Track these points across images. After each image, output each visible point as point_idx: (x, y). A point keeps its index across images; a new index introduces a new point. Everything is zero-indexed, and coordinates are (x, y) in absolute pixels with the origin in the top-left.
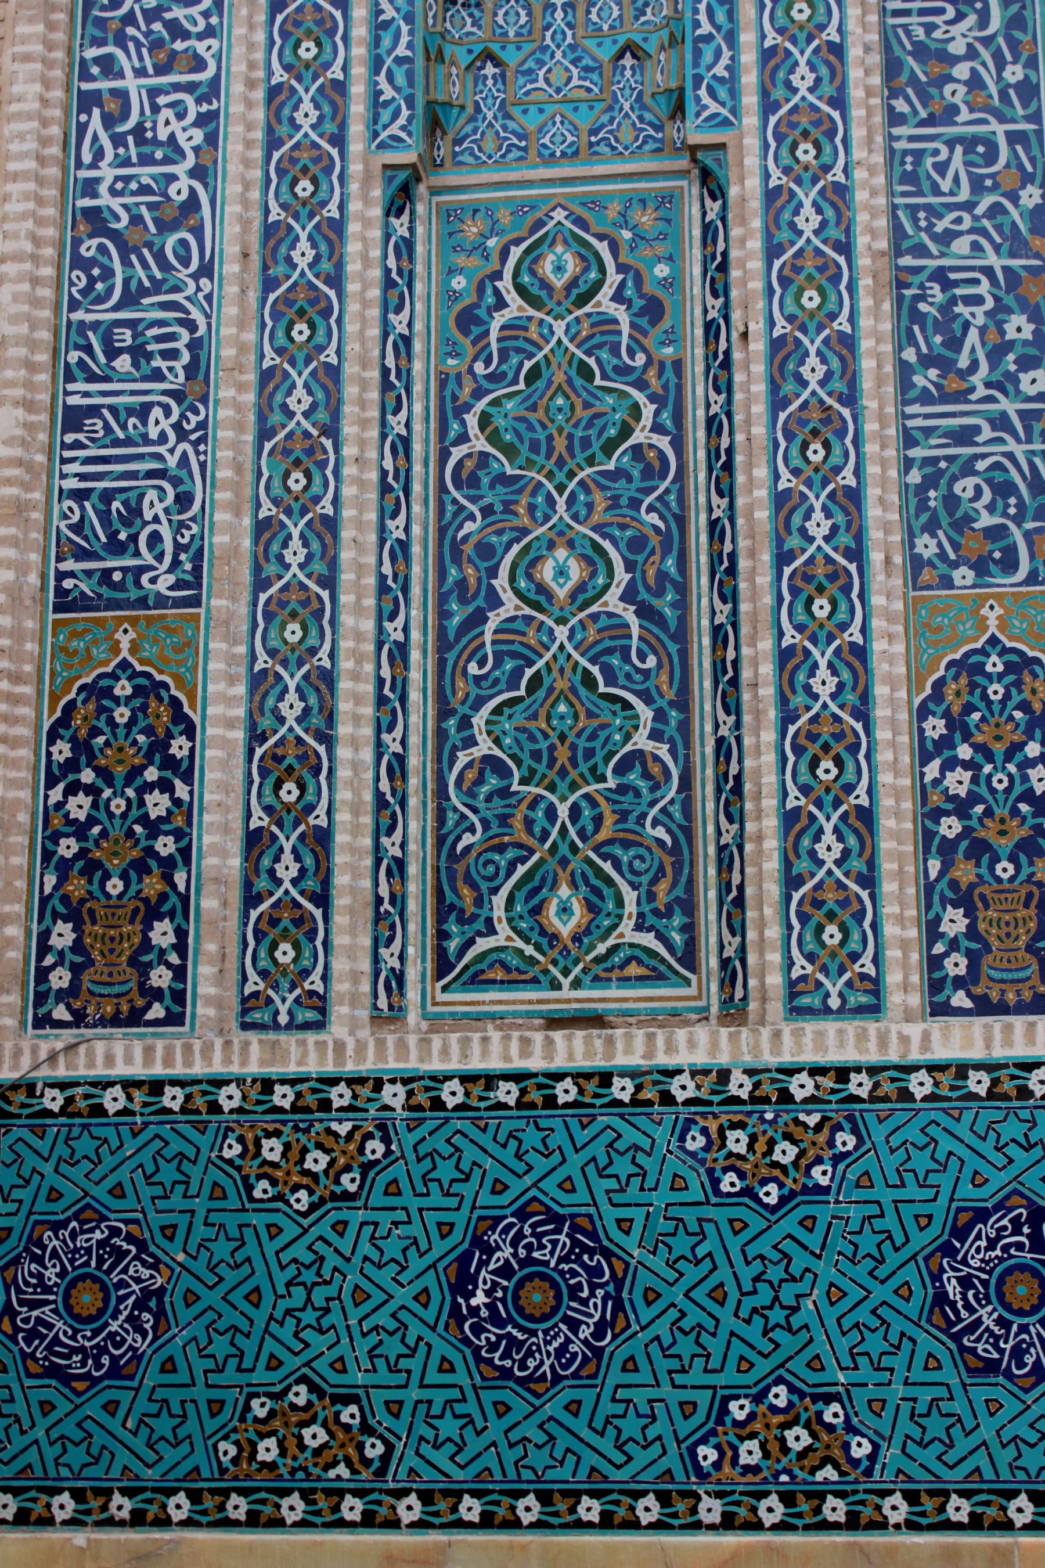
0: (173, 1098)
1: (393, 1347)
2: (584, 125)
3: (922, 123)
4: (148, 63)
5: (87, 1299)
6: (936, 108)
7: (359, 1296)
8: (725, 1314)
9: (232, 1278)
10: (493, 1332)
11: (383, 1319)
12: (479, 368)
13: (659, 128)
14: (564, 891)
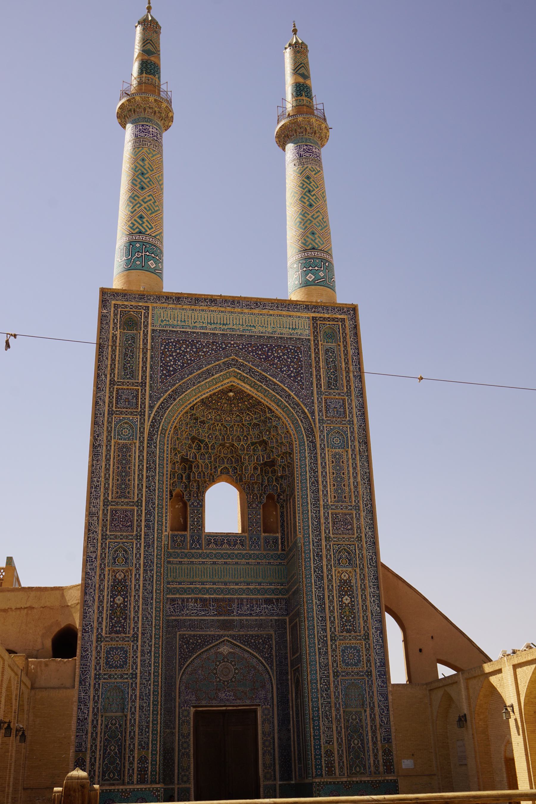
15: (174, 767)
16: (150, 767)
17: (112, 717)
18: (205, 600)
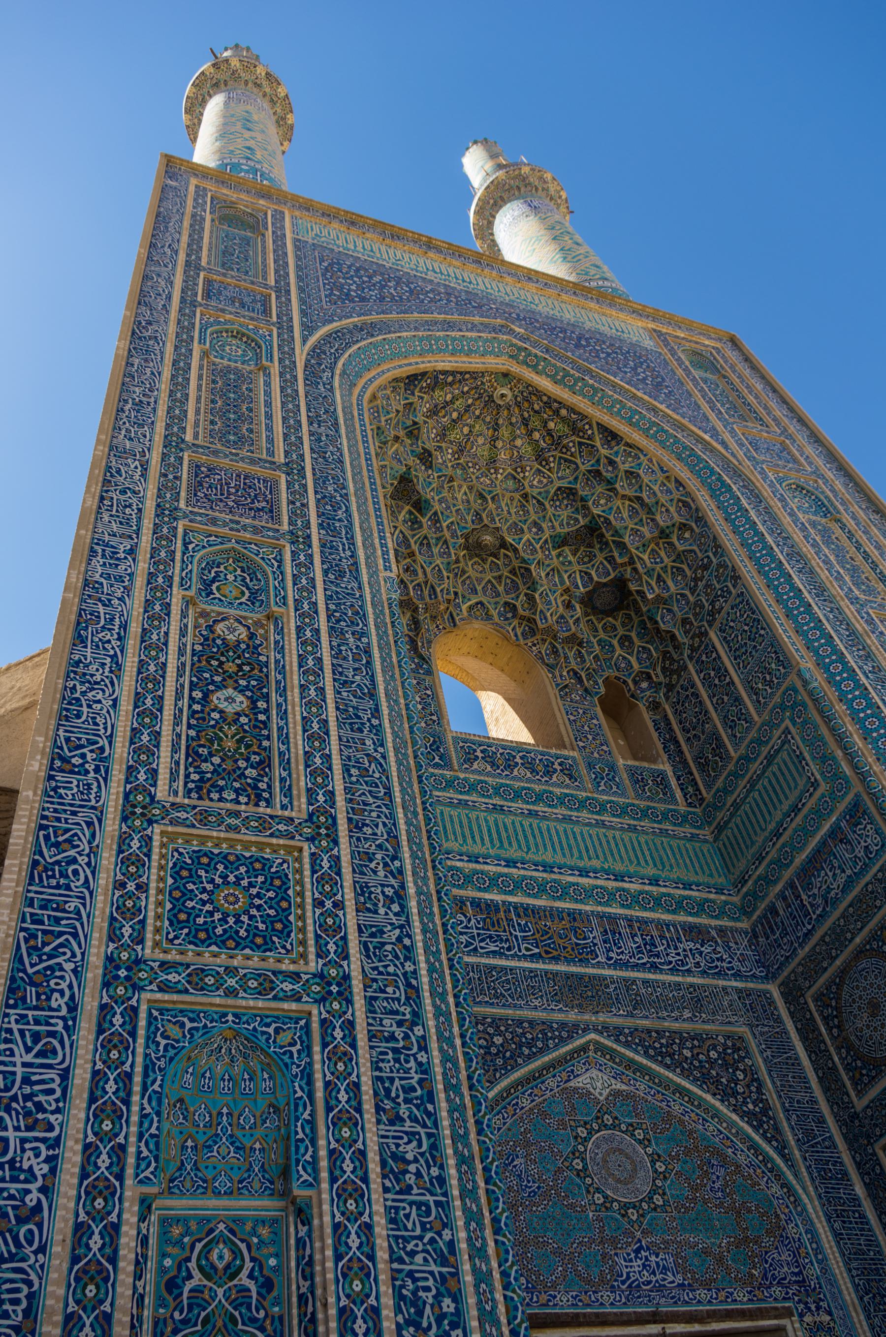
2: (236, 1179)
3: (397, 1193)
4: (22, 1124)
6: (403, 1185)
12: (177, 1315)
13: (272, 1183)
17: (207, 1225)
18: (491, 908)
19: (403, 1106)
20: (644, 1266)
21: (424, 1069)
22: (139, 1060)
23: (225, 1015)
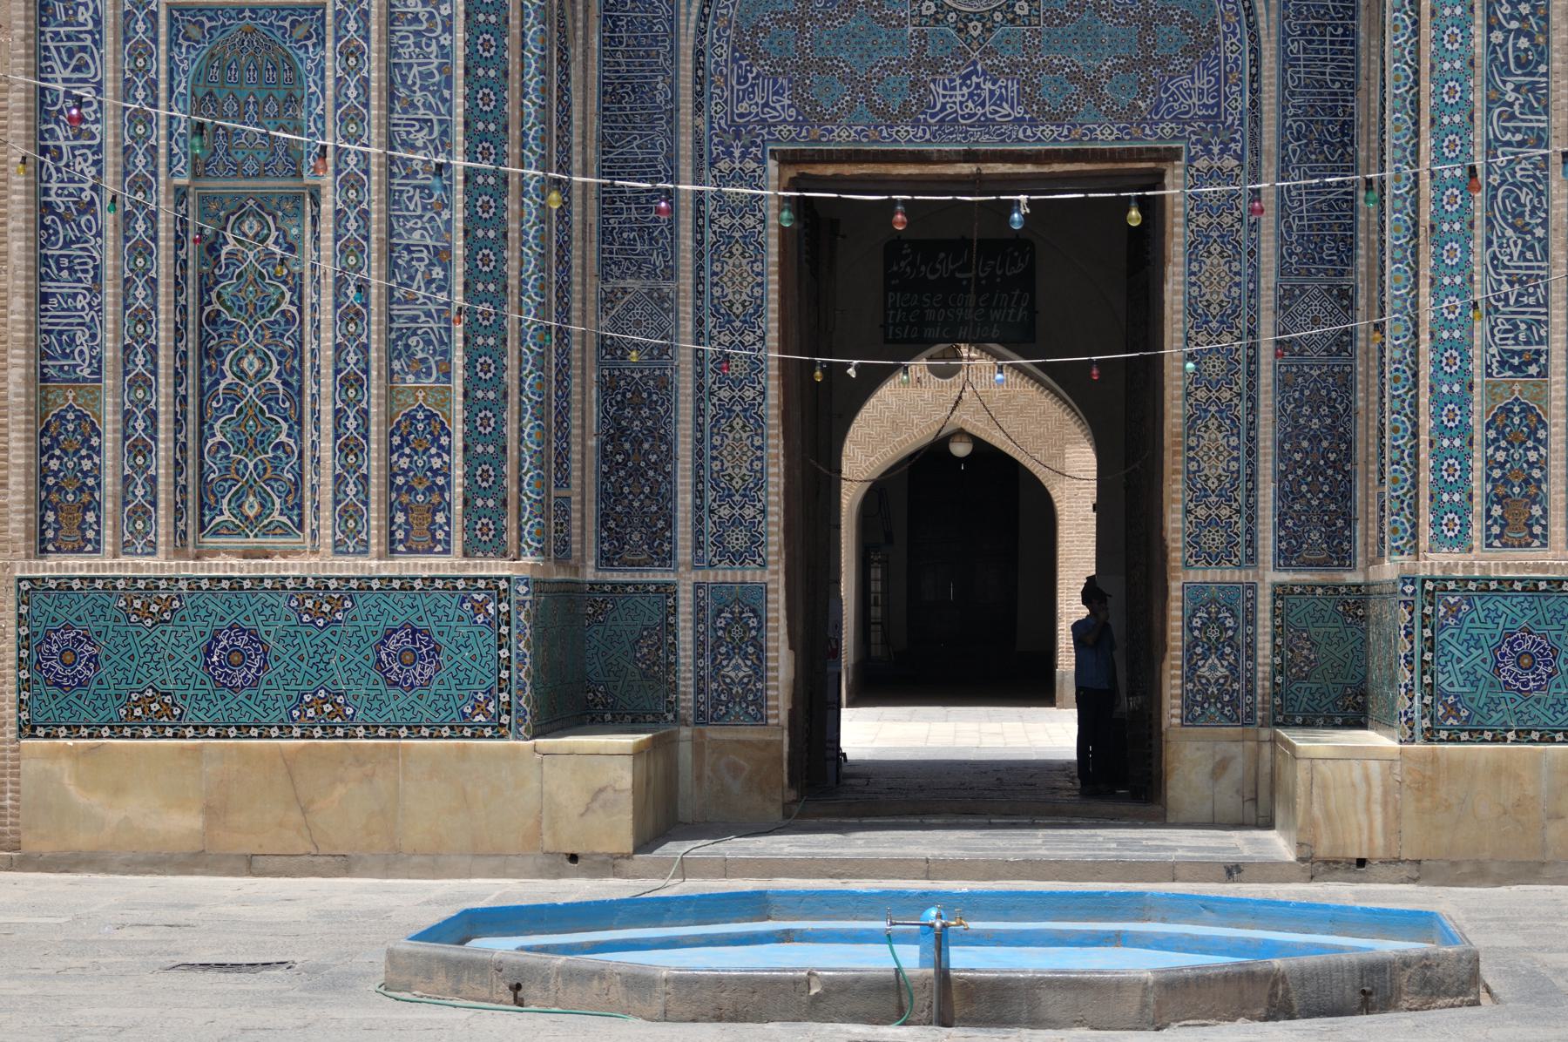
0: (99, 584)
1: (183, 676)
5: (68, 658)
7: (171, 657)
8: (303, 665)
9: (123, 650)
10: (220, 670)
11: (180, 665)
14: (251, 498)
15: (669, 477)
16: (458, 473)
19: (419, 94)
20: (971, 95)
21: (445, 52)
22: (163, 67)
23: (242, 11)
